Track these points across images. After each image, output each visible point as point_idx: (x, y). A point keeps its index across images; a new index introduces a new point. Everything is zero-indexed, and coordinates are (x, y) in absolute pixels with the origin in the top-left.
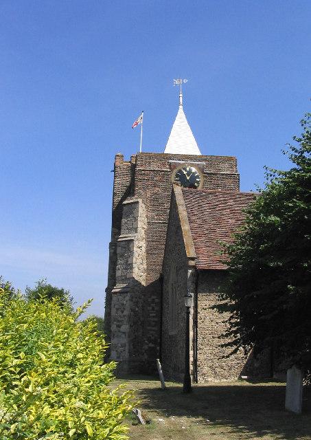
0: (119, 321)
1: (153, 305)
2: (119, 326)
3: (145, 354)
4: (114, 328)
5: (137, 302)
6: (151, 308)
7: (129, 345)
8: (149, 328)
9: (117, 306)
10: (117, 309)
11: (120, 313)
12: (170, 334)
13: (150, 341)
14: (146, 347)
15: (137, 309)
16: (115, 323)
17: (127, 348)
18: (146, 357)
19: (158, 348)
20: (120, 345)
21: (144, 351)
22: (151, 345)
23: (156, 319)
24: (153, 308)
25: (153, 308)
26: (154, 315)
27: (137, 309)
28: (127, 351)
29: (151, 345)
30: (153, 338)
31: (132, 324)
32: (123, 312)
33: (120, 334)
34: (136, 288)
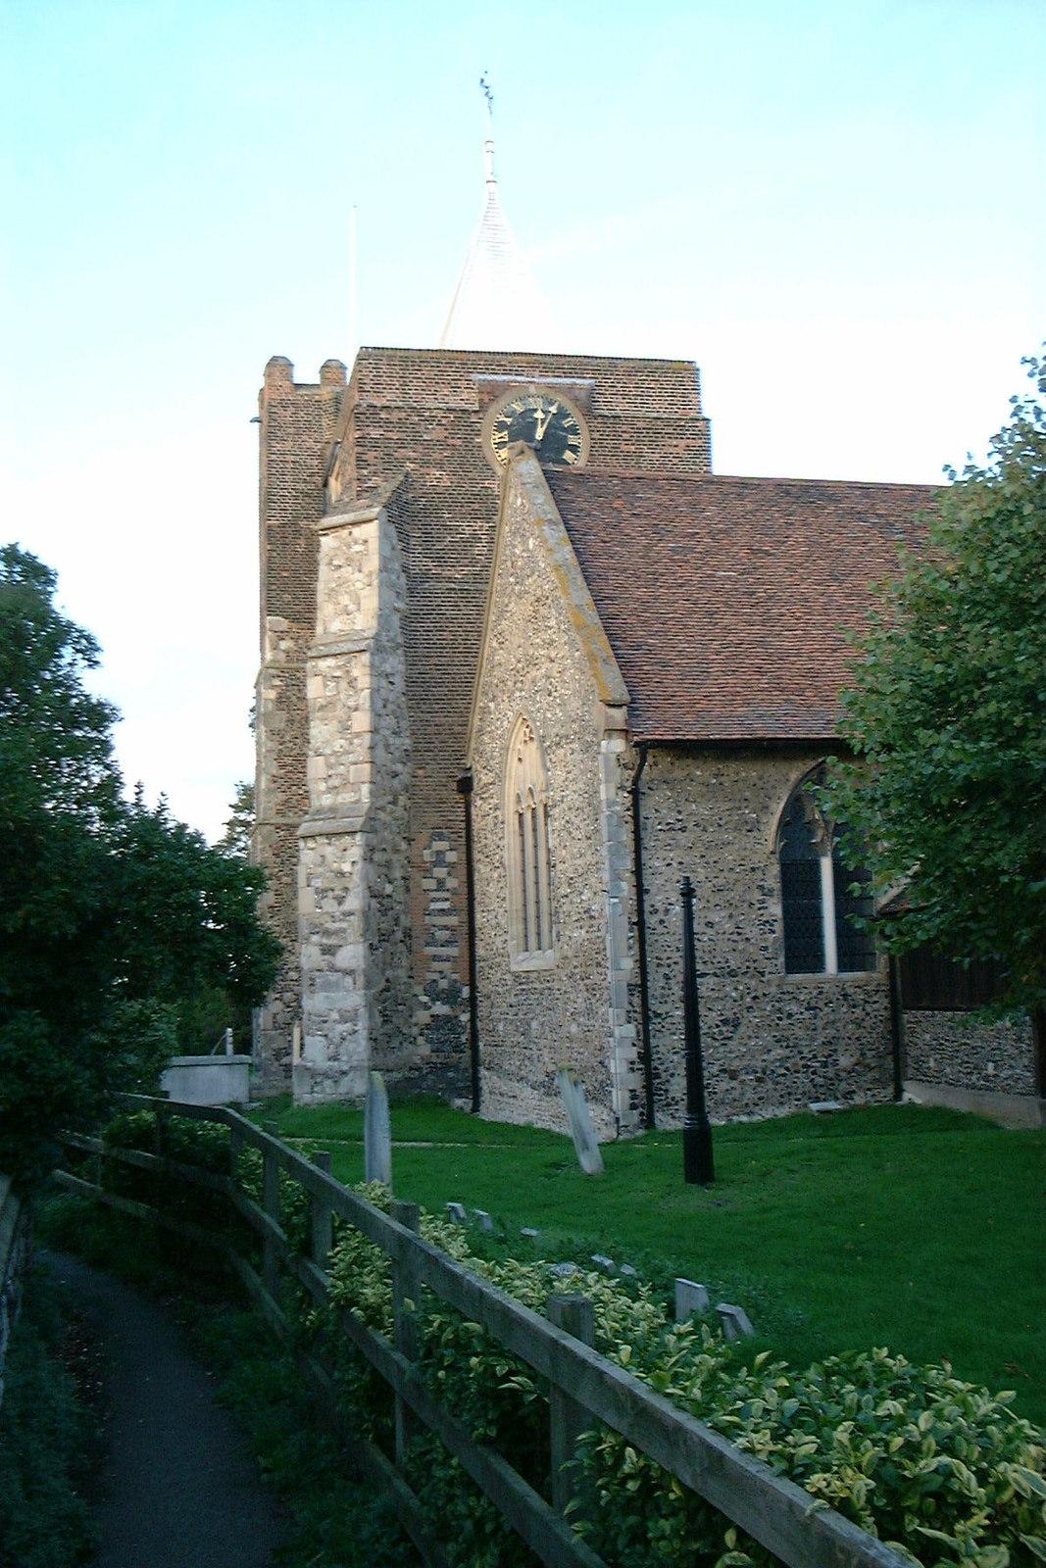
0: (327, 933)
1: (440, 872)
2: (328, 951)
3: (421, 1040)
4: (874, 697)
5: (388, 865)
6: (431, 884)
7: (371, 1017)
8: (431, 950)
9: (318, 883)
10: (322, 892)
11: (330, 905)
12: (514, 968)
13: (436, 996)
14: (423, 1017)
15: (389, 888)
16: (315, 938)
17: (362, 1026)
18: (424, 1049)
19: (465, 1018)
20: (335, 1016)
21: (415, 1031)
22: (441, 1009)
23: (453, 920)
24: (441, 883)
25: (441, 883)
26: (446, 905)
27: (389, 888)
28: (363, 1034)
29: (441, 1009)
30: (443, 984)
31: (376, 942)
32: (340, 900)
33: (334, 977)
34: (382, 815)
